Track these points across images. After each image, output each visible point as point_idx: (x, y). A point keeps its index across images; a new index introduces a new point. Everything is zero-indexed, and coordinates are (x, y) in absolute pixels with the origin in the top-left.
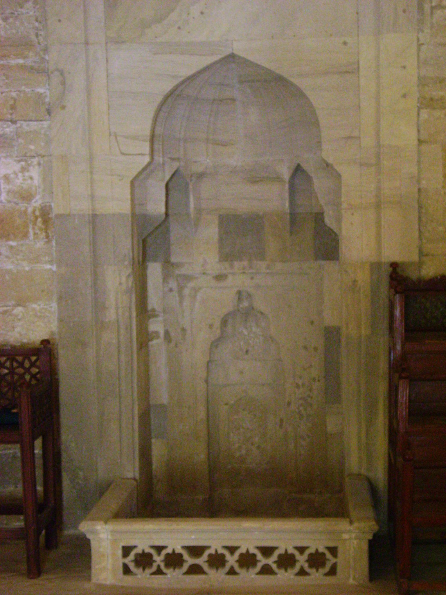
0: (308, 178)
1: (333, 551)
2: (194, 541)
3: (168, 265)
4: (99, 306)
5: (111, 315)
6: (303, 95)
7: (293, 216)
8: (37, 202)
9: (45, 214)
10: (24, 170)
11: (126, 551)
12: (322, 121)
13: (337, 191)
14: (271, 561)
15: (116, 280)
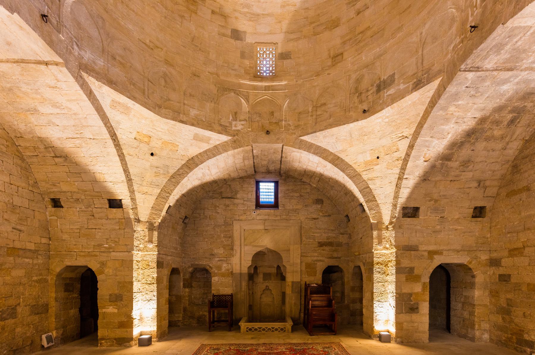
3: (253, 282)
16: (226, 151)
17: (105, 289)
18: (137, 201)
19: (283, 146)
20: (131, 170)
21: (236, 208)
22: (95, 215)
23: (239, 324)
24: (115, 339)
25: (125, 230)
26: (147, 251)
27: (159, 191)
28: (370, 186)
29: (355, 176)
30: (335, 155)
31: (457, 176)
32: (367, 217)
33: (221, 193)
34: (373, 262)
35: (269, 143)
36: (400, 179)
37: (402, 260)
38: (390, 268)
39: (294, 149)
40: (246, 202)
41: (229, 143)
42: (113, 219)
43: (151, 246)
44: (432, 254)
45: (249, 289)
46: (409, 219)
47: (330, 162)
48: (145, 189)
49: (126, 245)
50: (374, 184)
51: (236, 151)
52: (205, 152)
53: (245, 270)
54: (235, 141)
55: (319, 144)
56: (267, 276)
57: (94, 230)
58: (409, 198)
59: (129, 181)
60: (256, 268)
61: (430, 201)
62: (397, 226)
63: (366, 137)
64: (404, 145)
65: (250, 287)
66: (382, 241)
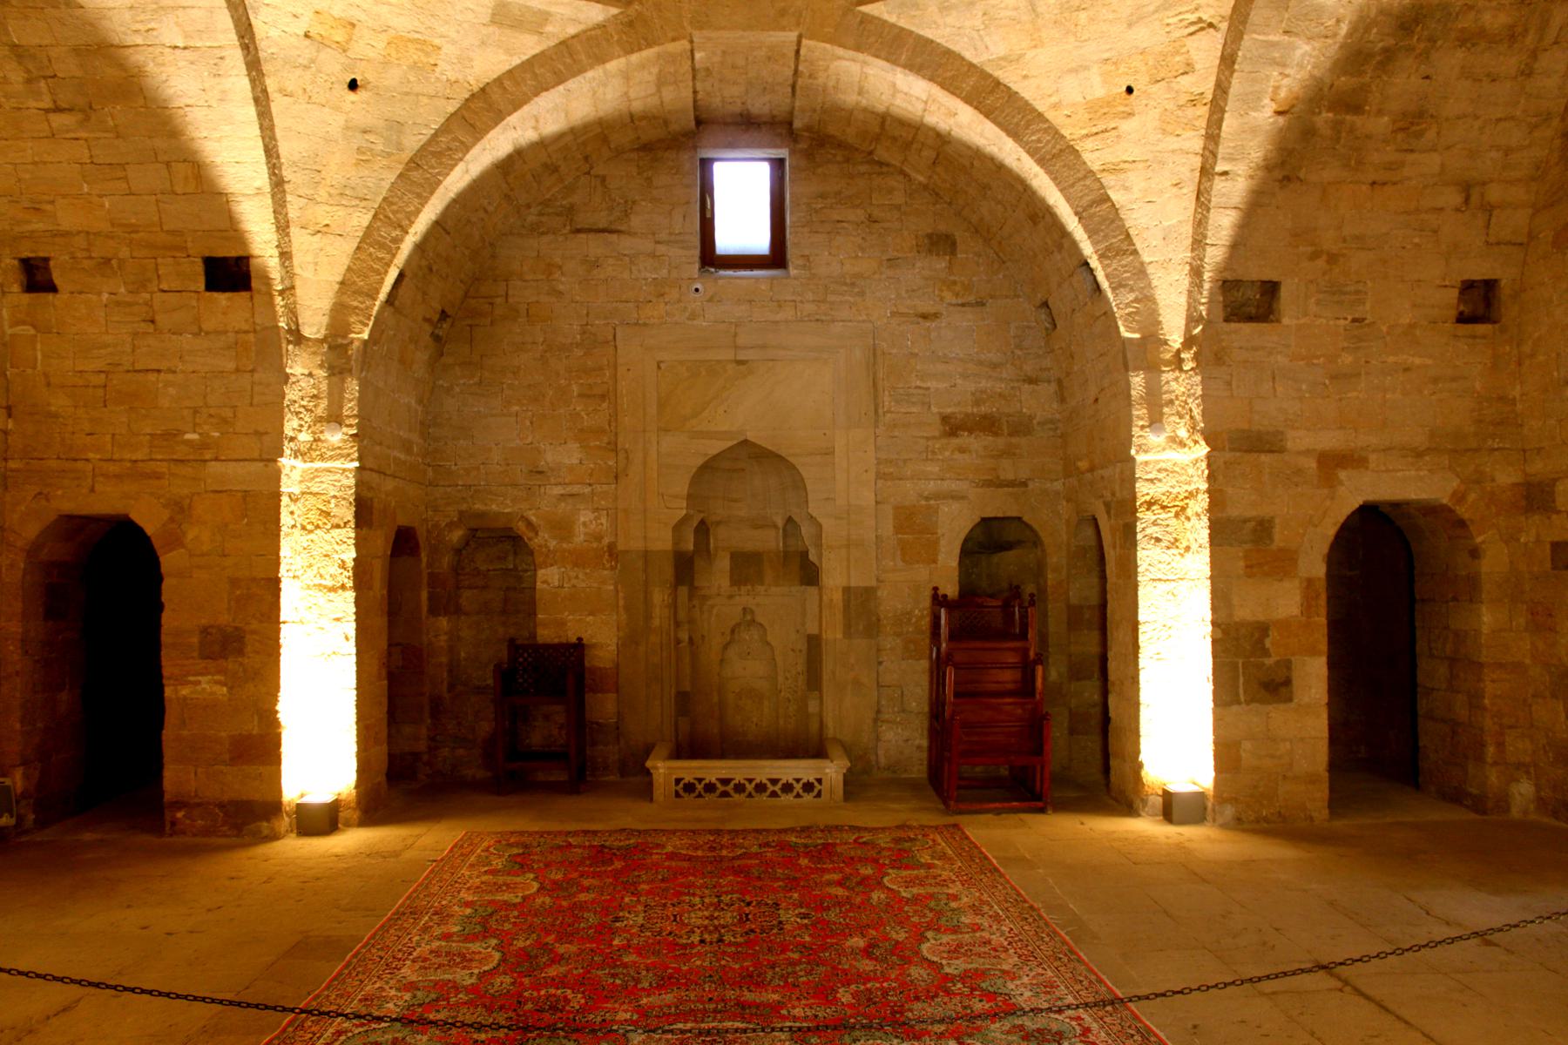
0: (797, 527)
1: (819, 781)
2: (725, 774)
3: (693, 589)
4: (648, 617)
5: (656, 622)
6: (794, 467)
7: (786, 553)
8: (606, 541)
9: (611, 548)
10: (596, 518)
11: (678, 781)
12: (809, 487)
13: (819, 536)
14: (777, 788)
15: (659, 597)
16: (601, 60)
17: (182, 612)
18: (296, 261)
19: (800, 37)
20: (285, 148)
21: (626, 275)
22: (157, 318)
23: (649, 764)
24: (221, 806)
25: (256, 376)
26: (322, 458)
27: (366, 219)
28: (1114, 196)
29: (1059, 155)
30: (985, 76)
31: (1390, 167)
32: (1108, 315)
33: (571, 210)
34: (1134, 499)
35: (750, 28)
36: (1206, 172)
37: (1230, 490)
38: (1194, 519)
39: (840, 51)
40: (662, 249)
41: (611, 29)
42: (217, 332)
43: (335, 437)
44: (1332, 463)
45: (678, 624)
46: (1247, 328)
47: (968, 100)
48: (322, 214)
49: (257, 433)
50: (1126, 189)
51: (635, 58)
52: (528, 65)
53: (662, 541)
54: (631, 24)
55: (928, 33)
56: (747, 567)
57: (152, 377)
58: (1237, 246)
59: (278, 183)
60: (703, 529)
61: (1314, 256)
62: (1208, 350)
63: (1083, 16)
64: (1206, 51)
65: (682, 615)
66: (1162, 414)
